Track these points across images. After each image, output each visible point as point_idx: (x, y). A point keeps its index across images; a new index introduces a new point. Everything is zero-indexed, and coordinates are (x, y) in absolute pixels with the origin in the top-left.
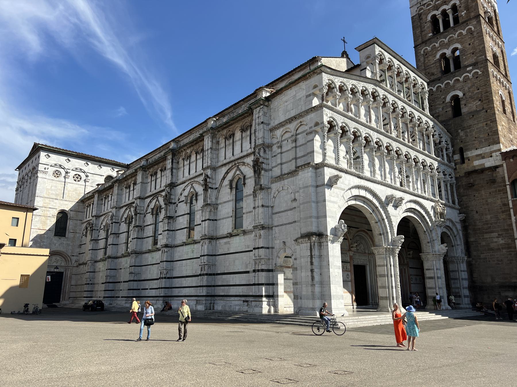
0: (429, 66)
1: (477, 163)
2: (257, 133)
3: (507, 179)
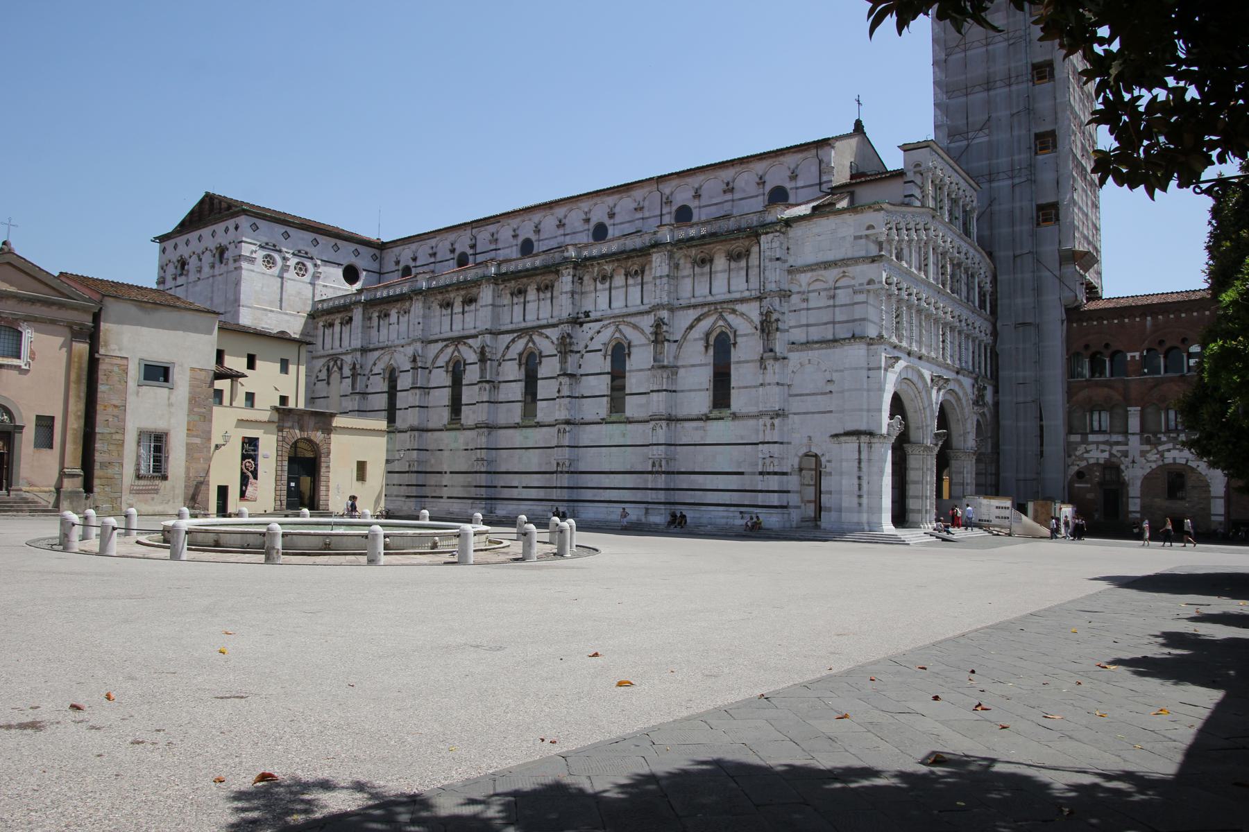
2: (767, 273)
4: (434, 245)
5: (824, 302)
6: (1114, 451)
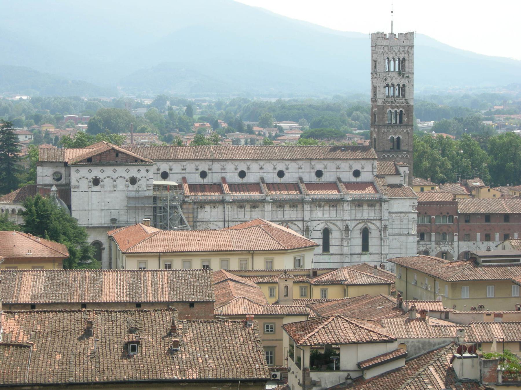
4: (185, 165)
5: (399, 223)
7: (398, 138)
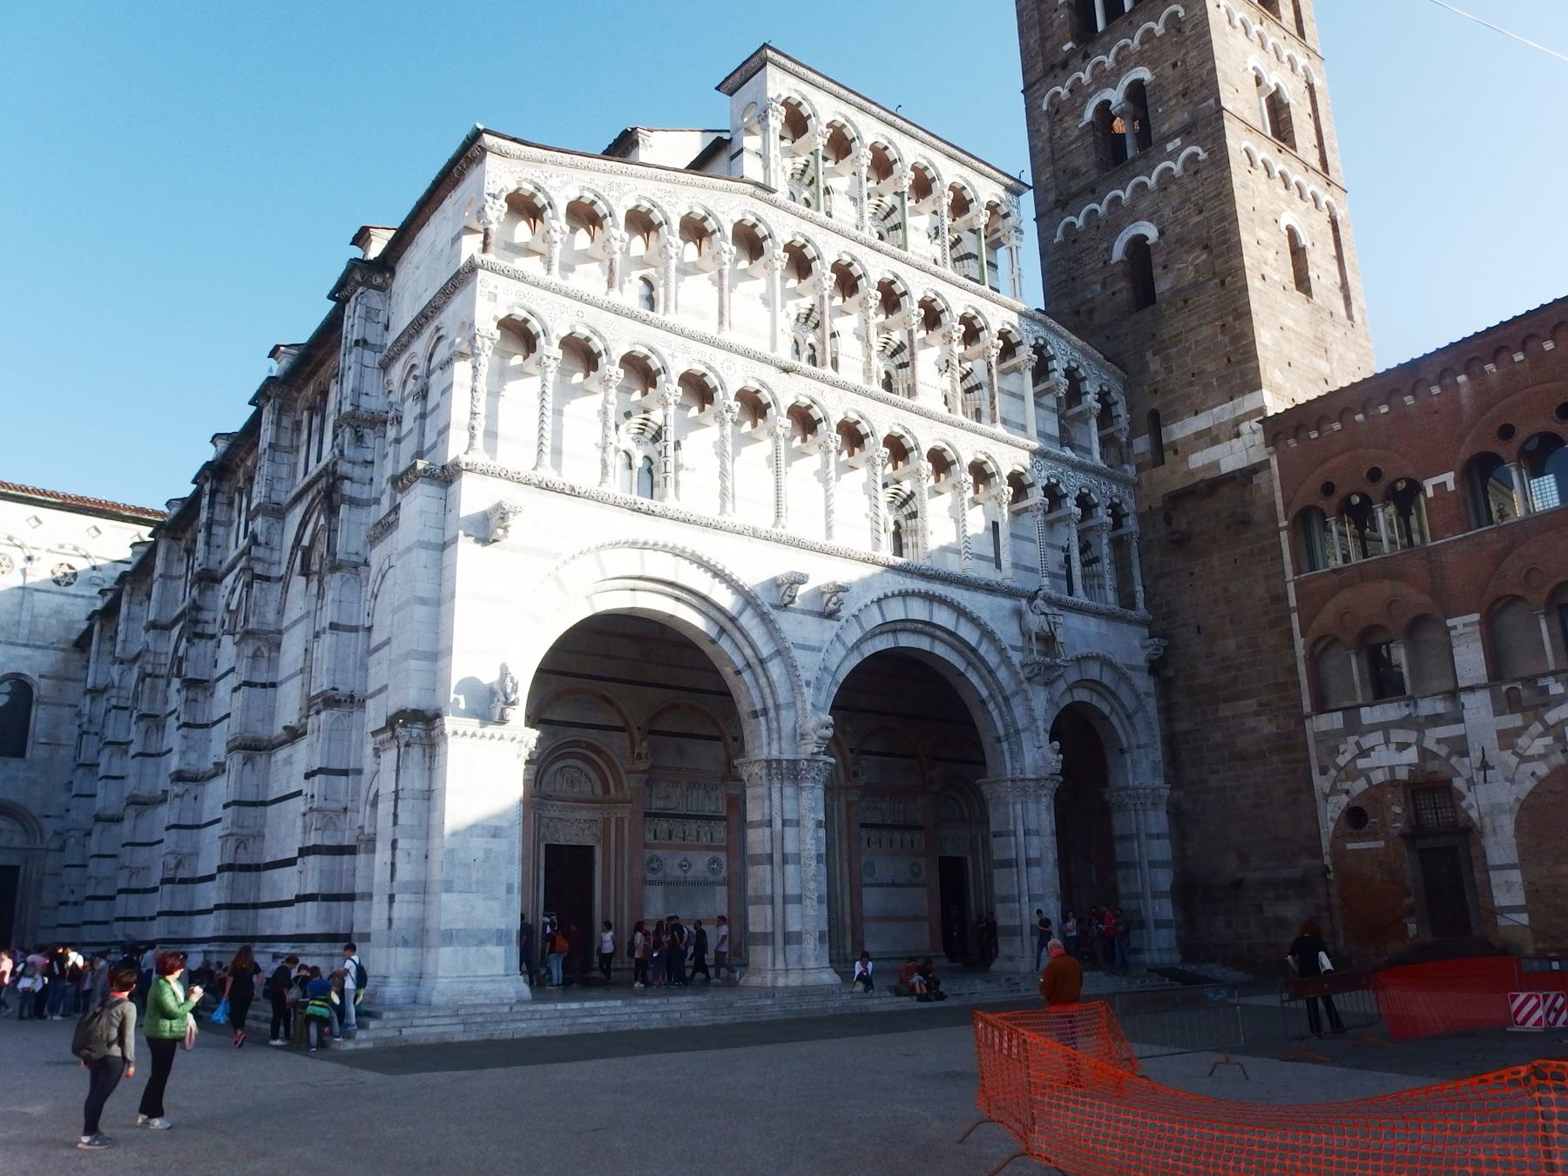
0: (1064, 147)
1: (1198, 460)
3: (1280, 508)
6: (1430, 744)
7: (1137, 92)
